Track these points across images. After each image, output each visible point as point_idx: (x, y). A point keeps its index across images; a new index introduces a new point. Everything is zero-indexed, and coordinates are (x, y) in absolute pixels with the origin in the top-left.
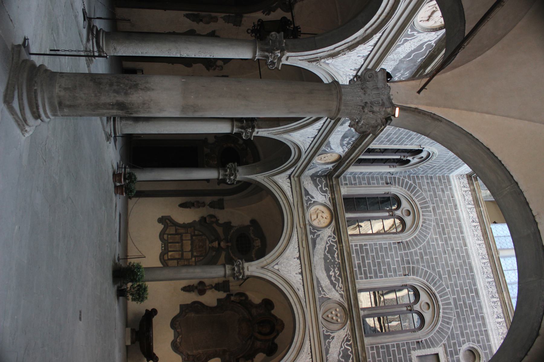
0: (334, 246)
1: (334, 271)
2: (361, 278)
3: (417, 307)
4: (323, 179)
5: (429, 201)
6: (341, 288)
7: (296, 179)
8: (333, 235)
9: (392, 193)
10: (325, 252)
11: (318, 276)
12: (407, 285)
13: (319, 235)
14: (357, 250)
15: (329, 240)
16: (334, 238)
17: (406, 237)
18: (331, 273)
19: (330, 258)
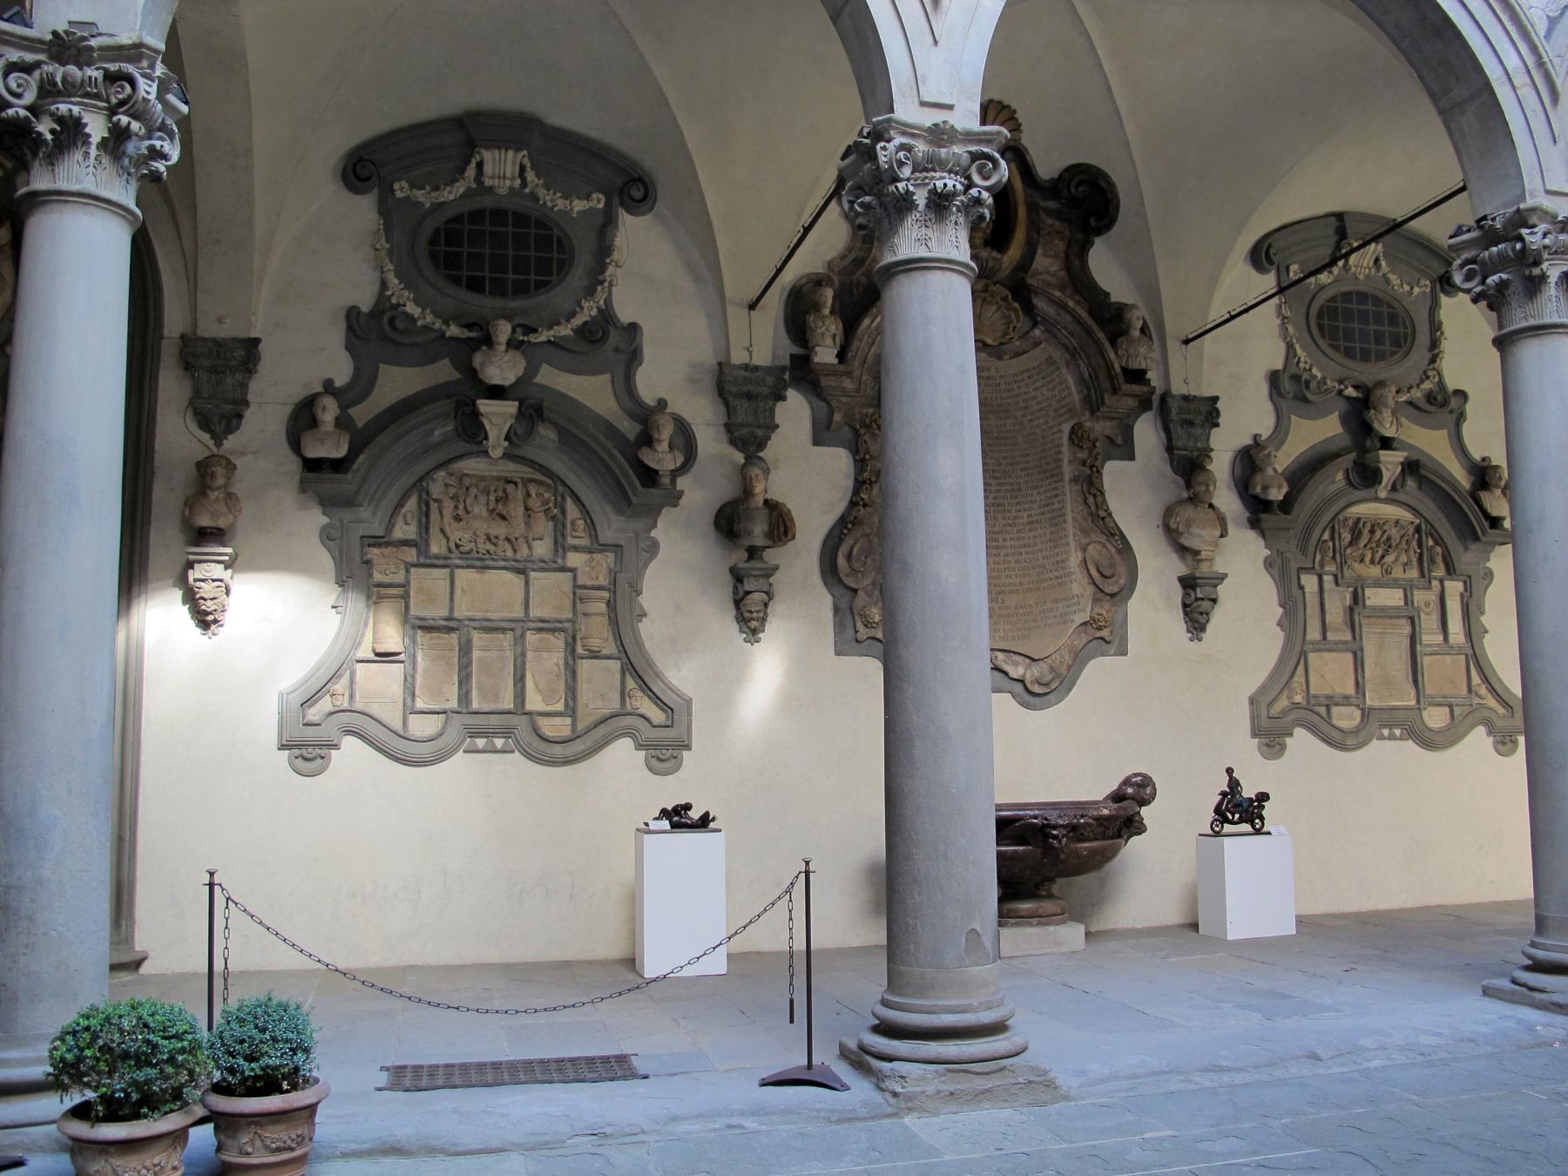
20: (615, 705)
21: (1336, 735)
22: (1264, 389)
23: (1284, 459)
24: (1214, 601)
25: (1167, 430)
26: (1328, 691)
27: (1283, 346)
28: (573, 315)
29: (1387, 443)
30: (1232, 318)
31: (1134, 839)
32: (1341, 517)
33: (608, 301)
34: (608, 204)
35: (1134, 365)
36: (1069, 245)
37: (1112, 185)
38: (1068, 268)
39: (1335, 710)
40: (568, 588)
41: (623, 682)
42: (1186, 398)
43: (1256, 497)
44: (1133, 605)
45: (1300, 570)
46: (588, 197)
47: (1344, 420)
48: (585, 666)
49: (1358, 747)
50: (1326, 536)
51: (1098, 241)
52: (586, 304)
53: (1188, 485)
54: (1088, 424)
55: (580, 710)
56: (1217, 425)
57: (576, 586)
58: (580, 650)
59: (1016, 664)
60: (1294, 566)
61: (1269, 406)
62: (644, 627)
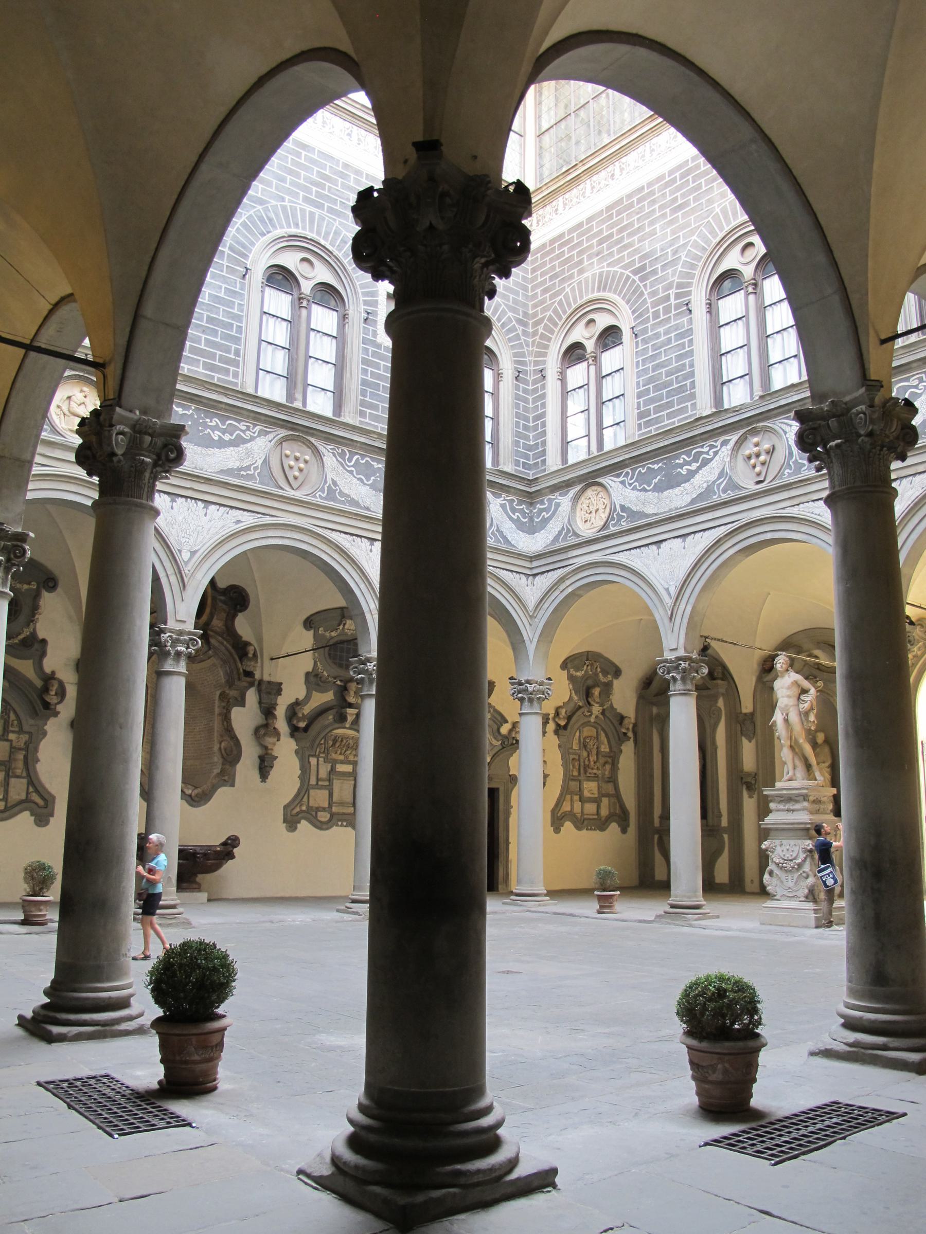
0: (640, 471)
1: (681, 467)
2: (694, 406)
3: (748, 272)
4: (535, 511)
5: (570, 284)
6: (712, 447)
7: (535, 564)
8: (621, 479)
9: (559, 366)
10: (649, 491)
11: (689, 500)
12: (707, 304)
13: (621, 505)
14: (648, 424)
15: (630, 485)
16: (627, 473)
17: (625, 324)
18: (684, 472)
19: (659, 477)
20: (23, 797)
21: (318, 824)
22: (303, 679)
23: (307, 710)
24: (272, 767)
25: (260, 695)
26: (317, 806)
27: (313, 661)
28: (20, 634)
29: (350, 706)
30: (289, 656)
31: (230, 862)
32: (329, 734)
33: (34, 630)
34: (38, 587)
35: (248, 669)
36: (228, 615)
37: (247, 595)
38: (226, 625)
39: (319, 814)
40: (8, 748)
41: (28, 789)
42: (269, 682)
43: (294, 725)
44: (239, 767)
45: (310, 756)
46: (29, 584)
47: (335, 694)
48: (13, 781)
49: (327, 829)
50: (322, 742)
51: (240, 614)
52: (25, 630)
53: (266, 719)
54: (227, 692)
55: (9, 799)
56: (281, 695)
57: (11, 747)
58: (11, 774)
59: (188, 789)
60: (307, 753)
61: (304, 687)
62: (39, 766)
